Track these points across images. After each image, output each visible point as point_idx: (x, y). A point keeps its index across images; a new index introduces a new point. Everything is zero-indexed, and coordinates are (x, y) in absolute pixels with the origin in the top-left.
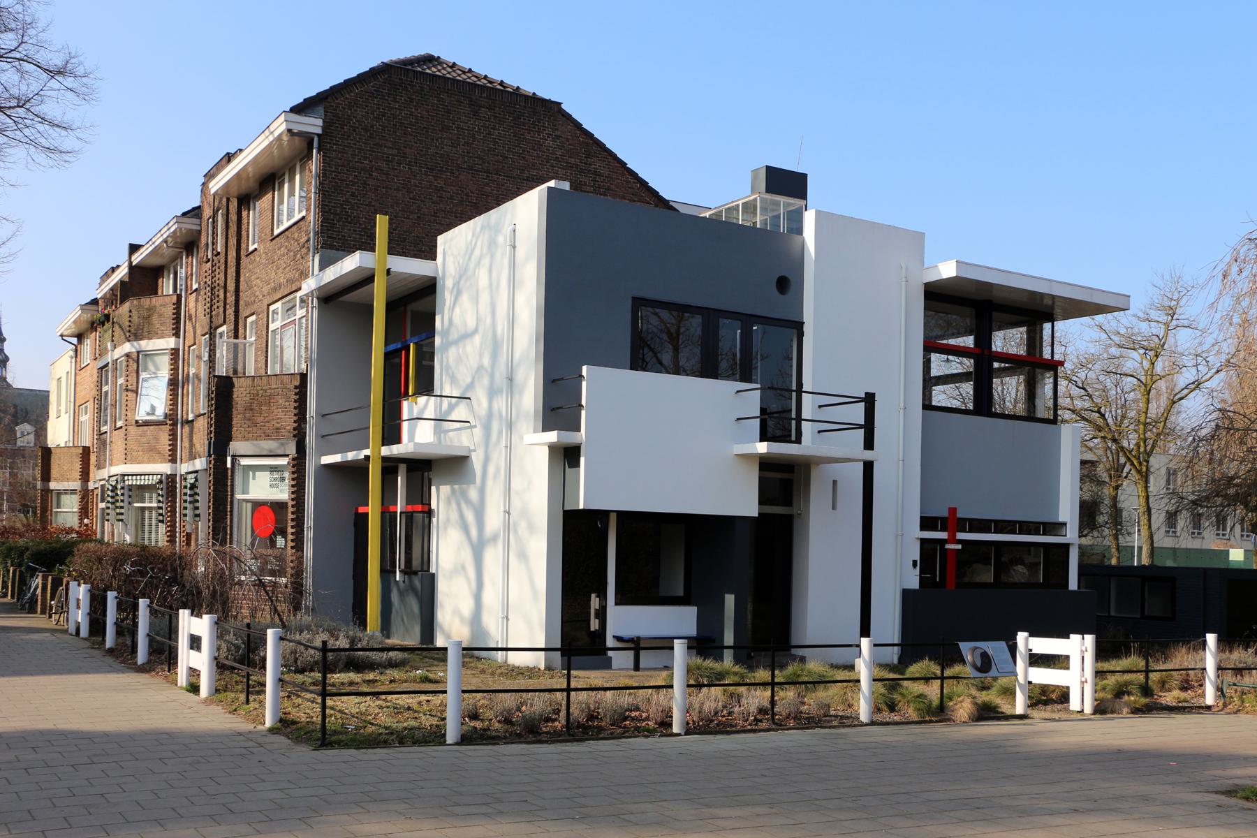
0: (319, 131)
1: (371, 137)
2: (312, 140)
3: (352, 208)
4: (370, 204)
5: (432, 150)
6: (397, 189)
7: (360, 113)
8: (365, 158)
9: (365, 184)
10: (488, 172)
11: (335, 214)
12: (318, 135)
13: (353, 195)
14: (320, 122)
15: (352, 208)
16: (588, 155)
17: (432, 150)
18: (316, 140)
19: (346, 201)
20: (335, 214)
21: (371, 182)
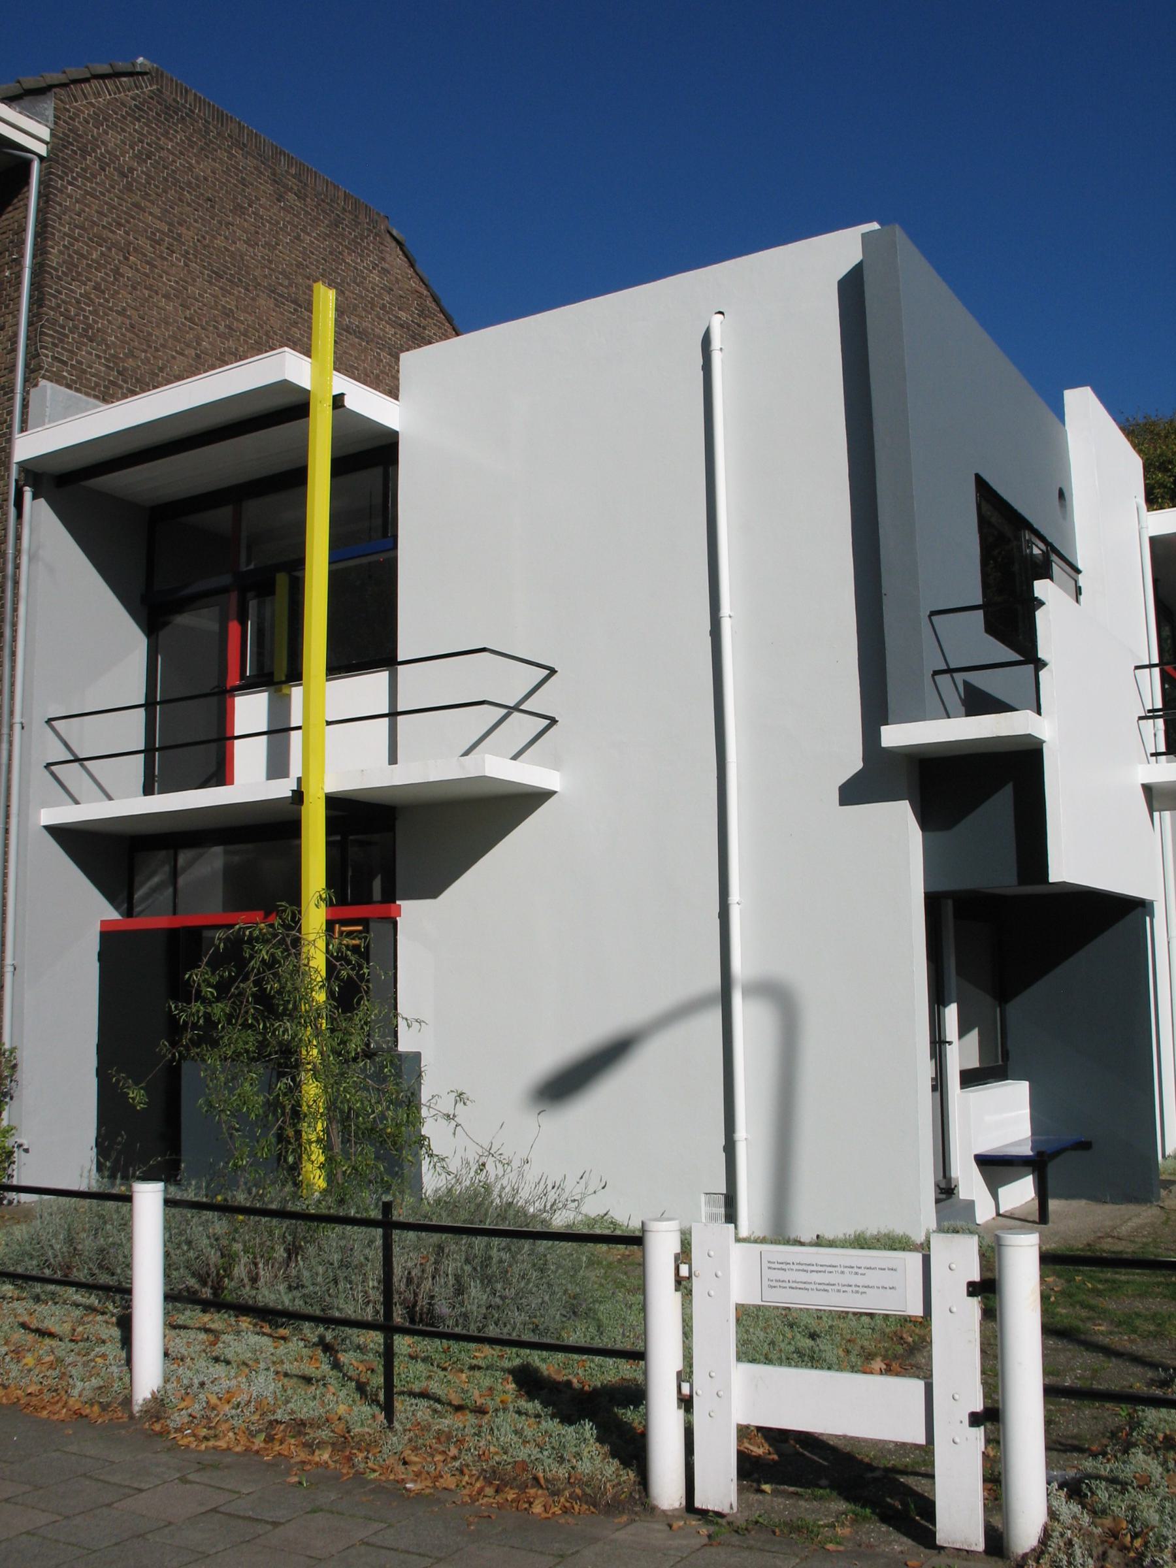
0: (42, 150)
1: (129, 188)
2: (27, 164)
3: (95, 312)
4: (122, 313)
5: (219, 242)
6: (166, 296)
7: (113, 139)
8: (119, 225)
9: (117, 272)
10: (295, 302)
11: (68, 318)
12: (41, 158)
13: (97, 287)
14: (45, 133)
15: (95, 312)
16: (422, 314)
17: (219, 242)
18: (36, 166)
19: (86, 295)
20: (68, 318)
21: (124, 269)
